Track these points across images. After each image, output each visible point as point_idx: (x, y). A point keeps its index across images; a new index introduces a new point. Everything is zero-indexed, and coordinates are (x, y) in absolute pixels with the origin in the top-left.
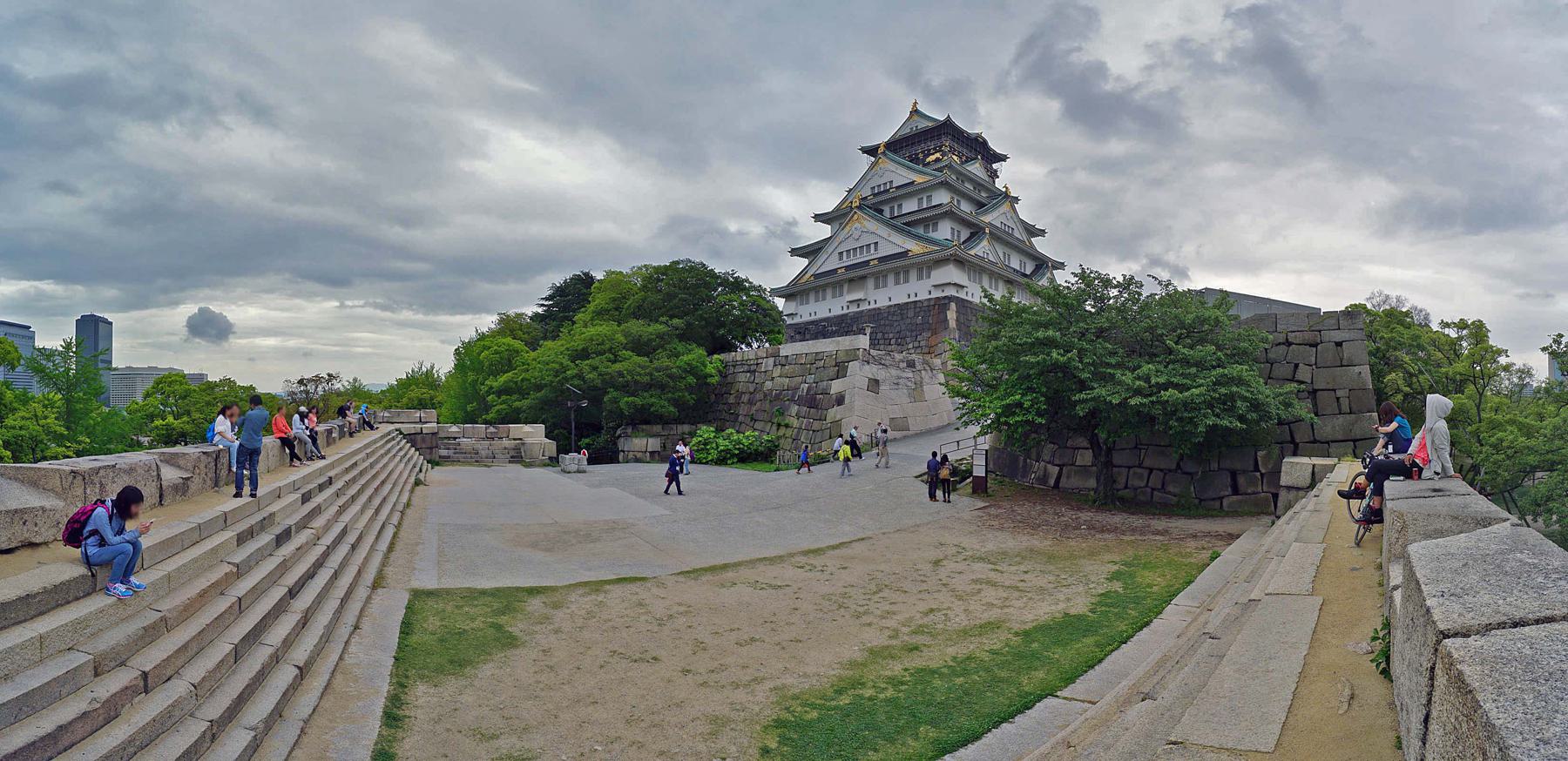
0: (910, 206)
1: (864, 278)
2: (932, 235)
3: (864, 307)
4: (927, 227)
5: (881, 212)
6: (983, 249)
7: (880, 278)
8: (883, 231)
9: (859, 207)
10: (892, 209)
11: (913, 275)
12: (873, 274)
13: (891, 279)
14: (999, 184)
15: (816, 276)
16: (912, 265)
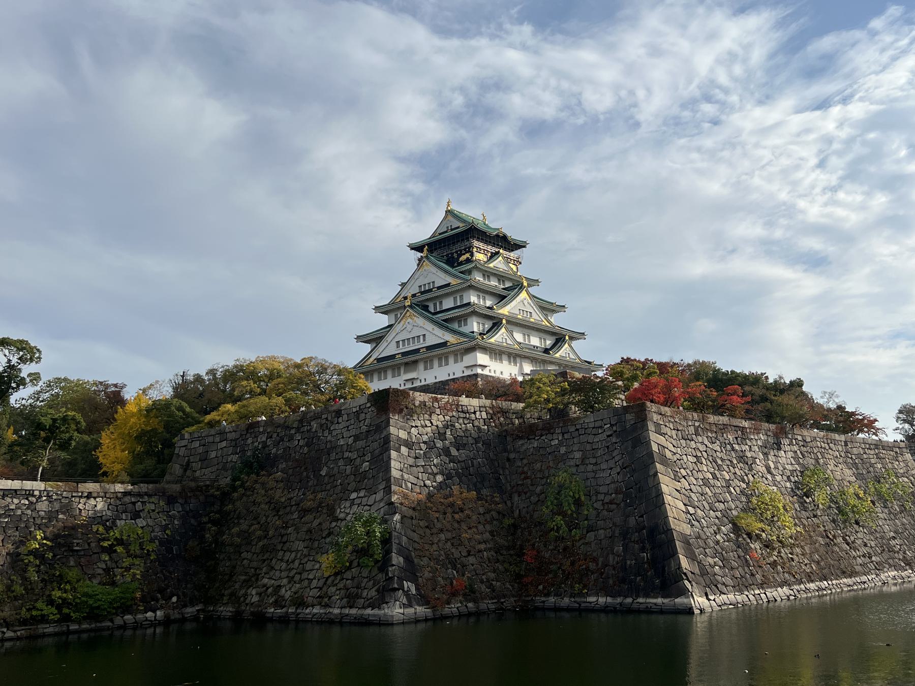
0: (448, 303)
1: (416, 362)
2: (465, 329)
3: (417, 384)
4: (460, 322)
5: (426, 308)
6: (500, 337)
7: (428, 363)
8: (429, 326)
9: (410, 306)
10: (435, 305)
11: (451, 360)
12: (421, 359)
13: (436, 363)
14: (523, 271)
15: (379, 360)
16: (449, 353)
